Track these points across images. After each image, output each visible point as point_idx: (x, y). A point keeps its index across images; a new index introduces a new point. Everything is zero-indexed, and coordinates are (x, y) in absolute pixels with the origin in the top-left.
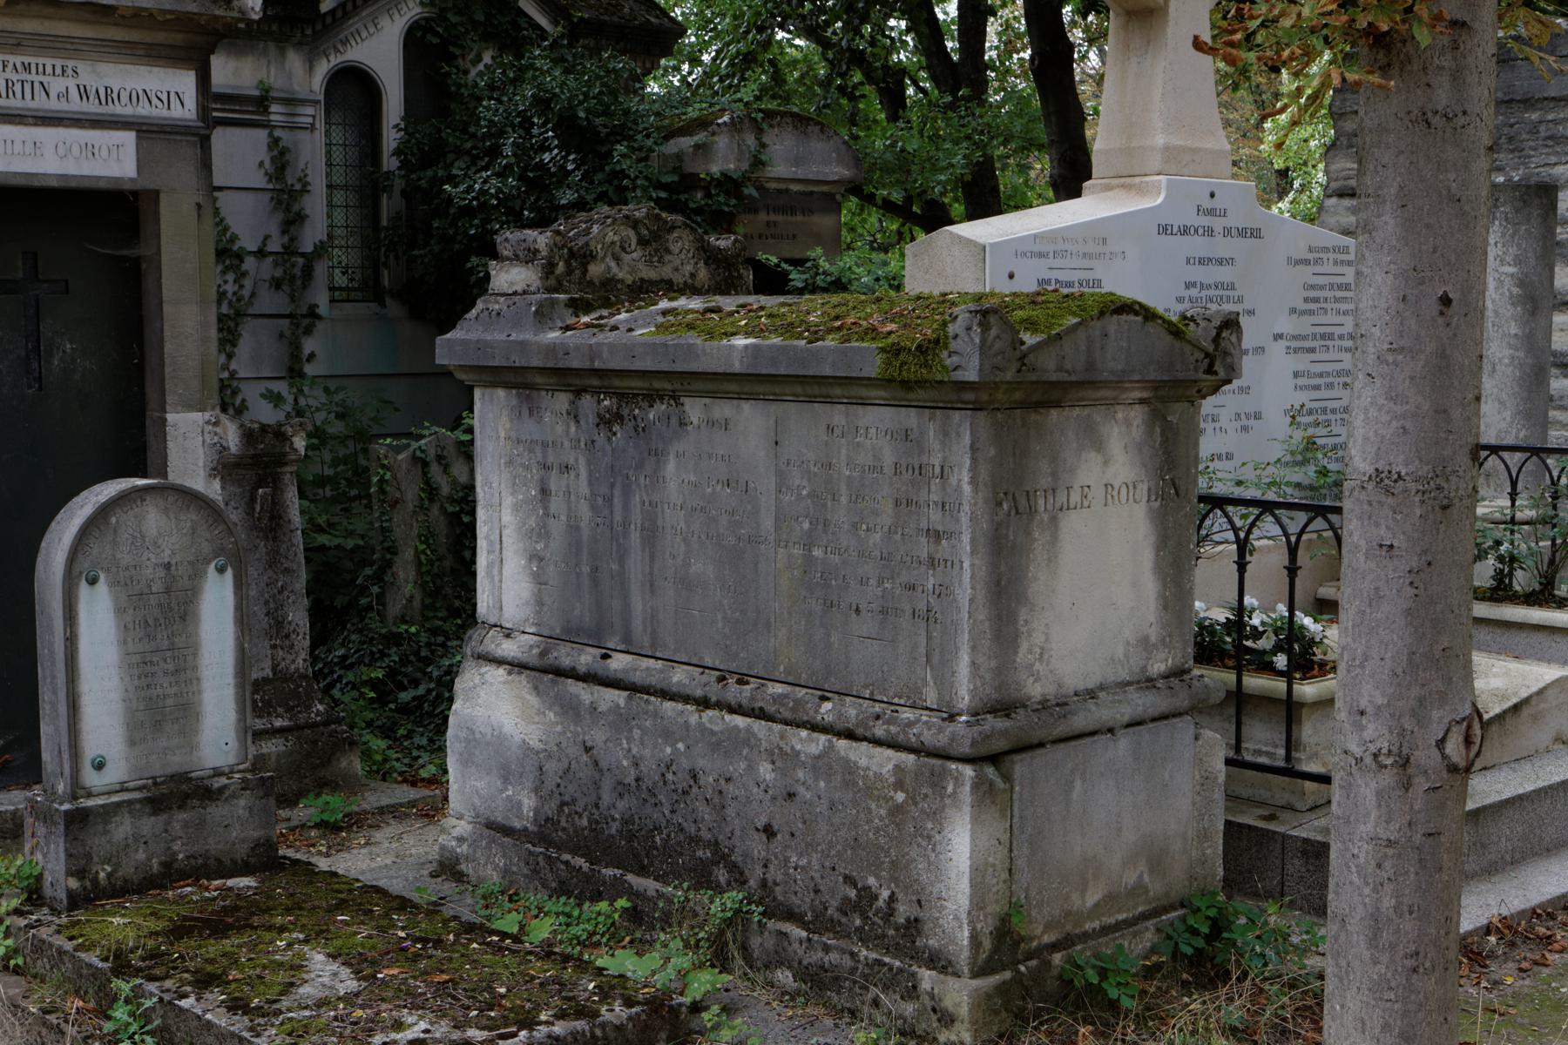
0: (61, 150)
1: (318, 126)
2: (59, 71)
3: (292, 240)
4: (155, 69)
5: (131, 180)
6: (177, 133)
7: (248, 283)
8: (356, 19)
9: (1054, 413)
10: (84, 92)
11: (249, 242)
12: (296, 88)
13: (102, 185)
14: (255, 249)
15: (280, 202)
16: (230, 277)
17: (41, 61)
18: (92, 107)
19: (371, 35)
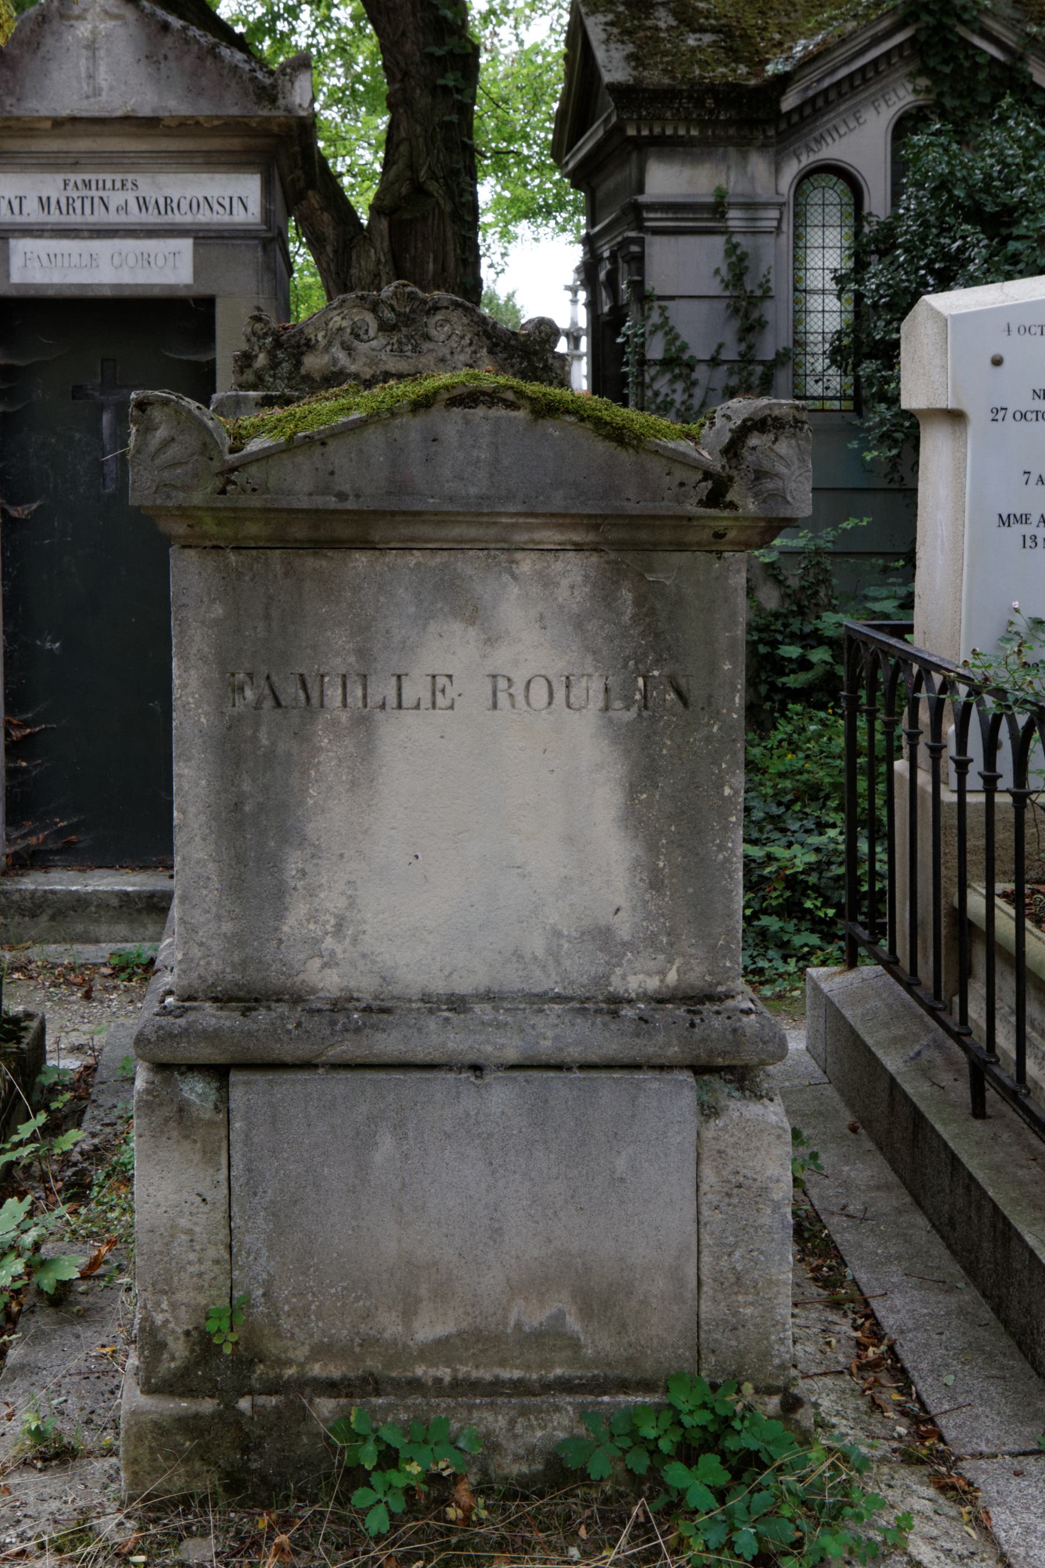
0: (117, 261)
1: (784, 228)
2: (118, 185)
3: (750, 347)
4: (217, 176)
5: (187, 286)
6: (233, 238)
7: (698, 393)
8: (832, 115)
9: (361, 560)
10: (143, 204)
11: (700, 350)
12: (759, 191)
13: (156, 292)
14: (707, 357)
15: (737, 311)
16: (679, 386)
17: (101, 177)
18: (151, 218)
19: (851, 130)
